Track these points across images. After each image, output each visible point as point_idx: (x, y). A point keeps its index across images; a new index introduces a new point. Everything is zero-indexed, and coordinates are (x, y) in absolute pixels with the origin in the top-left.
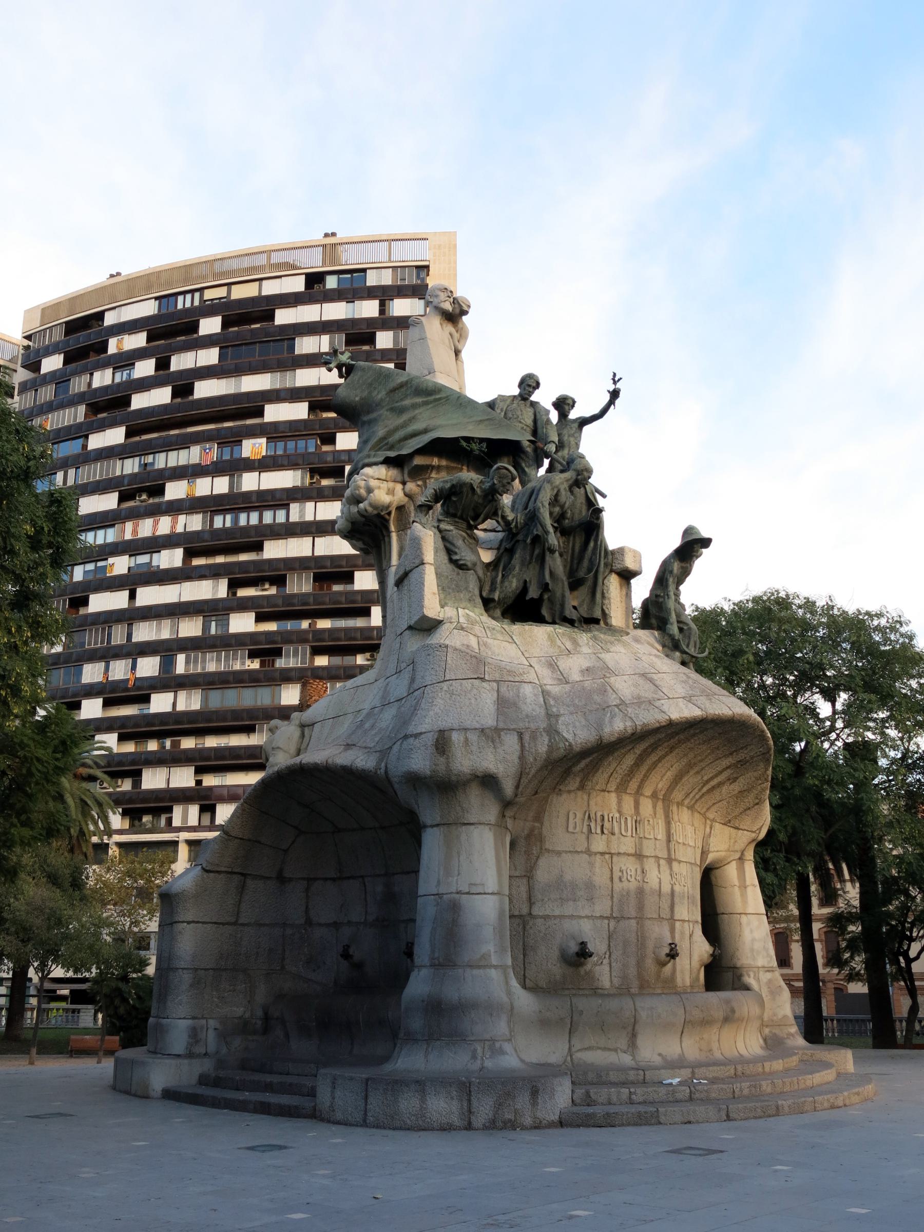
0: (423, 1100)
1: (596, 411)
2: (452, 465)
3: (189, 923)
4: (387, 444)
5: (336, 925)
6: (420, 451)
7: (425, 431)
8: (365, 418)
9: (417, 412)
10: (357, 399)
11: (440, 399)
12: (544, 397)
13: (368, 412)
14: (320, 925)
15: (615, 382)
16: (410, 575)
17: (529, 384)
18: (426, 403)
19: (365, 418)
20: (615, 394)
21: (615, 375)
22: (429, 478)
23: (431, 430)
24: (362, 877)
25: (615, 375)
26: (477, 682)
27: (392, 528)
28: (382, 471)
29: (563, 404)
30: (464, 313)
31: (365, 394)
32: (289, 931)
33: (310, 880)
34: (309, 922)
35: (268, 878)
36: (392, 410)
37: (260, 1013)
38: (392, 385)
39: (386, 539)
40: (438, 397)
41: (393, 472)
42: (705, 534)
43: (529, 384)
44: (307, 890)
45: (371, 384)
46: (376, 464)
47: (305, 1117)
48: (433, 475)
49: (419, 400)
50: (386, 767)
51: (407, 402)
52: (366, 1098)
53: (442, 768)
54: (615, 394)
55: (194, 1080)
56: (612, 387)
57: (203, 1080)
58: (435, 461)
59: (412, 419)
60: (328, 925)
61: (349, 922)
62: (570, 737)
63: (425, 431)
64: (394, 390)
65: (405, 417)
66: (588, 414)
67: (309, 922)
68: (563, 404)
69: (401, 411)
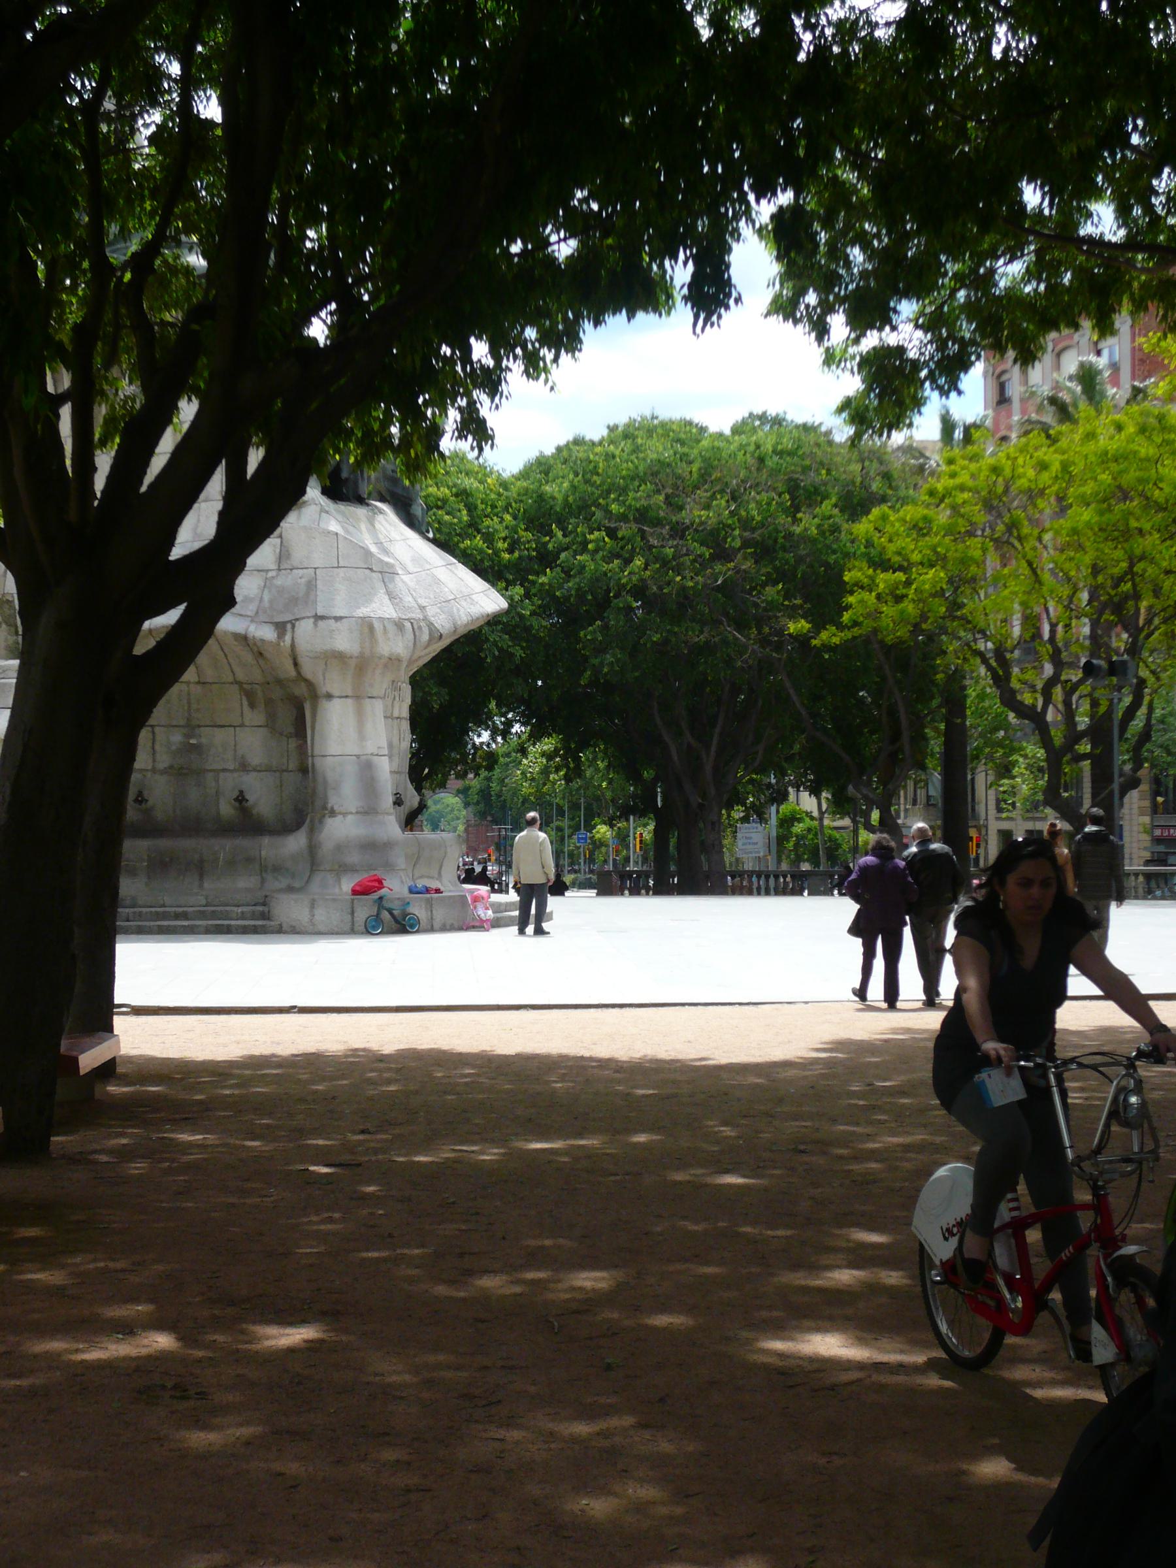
26: (367, 571)
47: (272, 932)
52: (353, 913)
53: (367, 652)
62: (439, 627)
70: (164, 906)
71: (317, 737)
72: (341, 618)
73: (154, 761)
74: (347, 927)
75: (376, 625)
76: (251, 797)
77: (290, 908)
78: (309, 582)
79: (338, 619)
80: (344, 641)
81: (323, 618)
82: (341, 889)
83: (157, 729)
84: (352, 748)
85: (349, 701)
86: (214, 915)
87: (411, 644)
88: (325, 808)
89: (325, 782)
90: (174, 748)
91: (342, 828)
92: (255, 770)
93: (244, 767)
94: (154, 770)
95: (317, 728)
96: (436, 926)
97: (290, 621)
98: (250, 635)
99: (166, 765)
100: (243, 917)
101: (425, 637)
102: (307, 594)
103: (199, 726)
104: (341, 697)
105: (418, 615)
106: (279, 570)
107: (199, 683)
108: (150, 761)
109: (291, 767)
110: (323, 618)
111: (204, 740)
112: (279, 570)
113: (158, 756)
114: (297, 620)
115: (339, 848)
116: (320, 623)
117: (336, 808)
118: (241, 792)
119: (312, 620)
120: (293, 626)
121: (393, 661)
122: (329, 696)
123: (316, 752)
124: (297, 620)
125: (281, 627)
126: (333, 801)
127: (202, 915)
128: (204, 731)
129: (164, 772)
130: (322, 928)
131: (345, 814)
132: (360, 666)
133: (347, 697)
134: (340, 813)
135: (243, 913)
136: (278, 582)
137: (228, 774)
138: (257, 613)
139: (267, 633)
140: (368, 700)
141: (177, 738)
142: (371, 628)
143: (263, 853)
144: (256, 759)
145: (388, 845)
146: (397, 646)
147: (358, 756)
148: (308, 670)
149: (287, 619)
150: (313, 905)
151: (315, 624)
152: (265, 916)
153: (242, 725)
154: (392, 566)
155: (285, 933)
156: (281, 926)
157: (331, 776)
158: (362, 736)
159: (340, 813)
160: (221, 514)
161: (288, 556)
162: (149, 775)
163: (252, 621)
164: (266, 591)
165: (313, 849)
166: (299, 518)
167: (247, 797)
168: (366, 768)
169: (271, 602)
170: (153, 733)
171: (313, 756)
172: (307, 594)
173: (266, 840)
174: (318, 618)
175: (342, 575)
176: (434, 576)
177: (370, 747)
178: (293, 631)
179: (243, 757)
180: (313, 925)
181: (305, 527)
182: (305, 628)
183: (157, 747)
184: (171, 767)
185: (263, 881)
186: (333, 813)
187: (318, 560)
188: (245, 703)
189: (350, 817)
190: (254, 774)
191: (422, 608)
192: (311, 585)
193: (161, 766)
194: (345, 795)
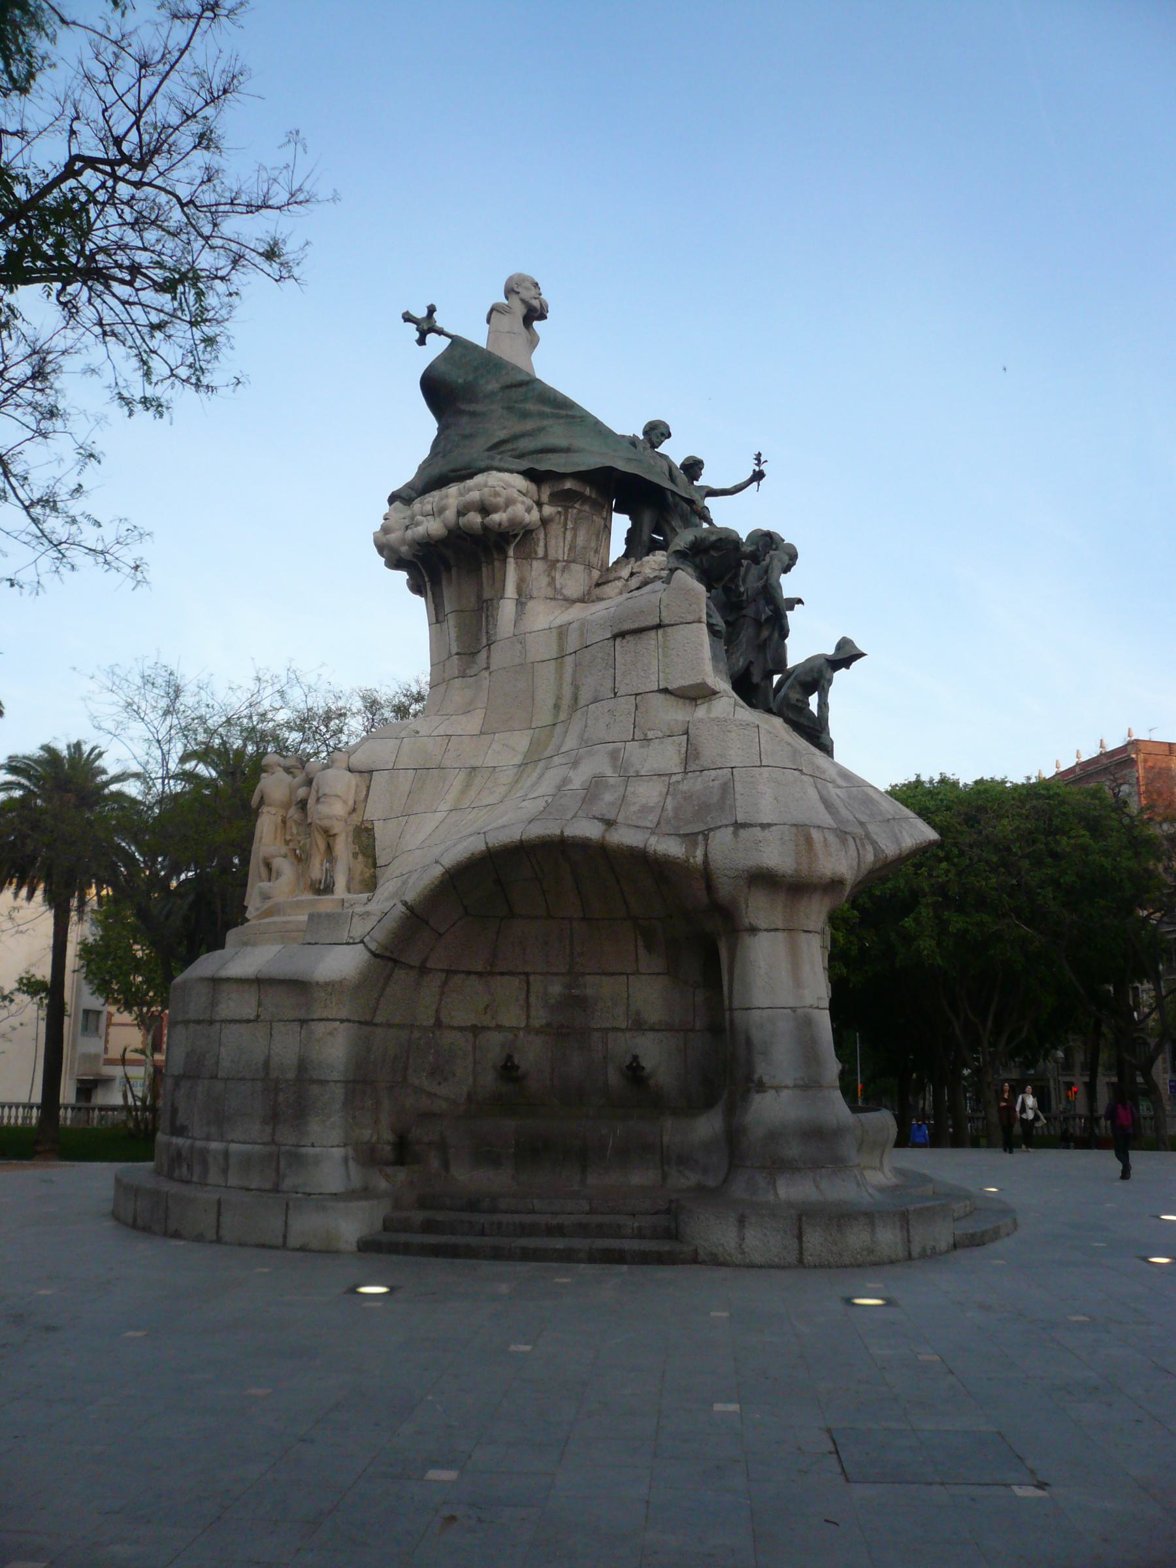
0: (873, 1233)
1: (728, 485)
2: (600, 500)
3: (342, 1021)
4: (513, 450)
5: (476, 1030)
6: (578, 476)
7: (567, 450)
8: (464, 407)
9: (545, 423)
10: (460, 381)
11: (573, 417)
12: (675, 451)
13: (471, 401)
14: (453, 1028)
15: (758, 465)
16: (669, 630)
17: (657, 432)
18: (558, 417)
19: (464, 407)
20: (758, 476)
21: (759, 454)
22: (572, 507)
23: (575, 452)
24: (527, 974)
25: (759, 454)
27: (511, 553)
28: (519, 482)
29: (693, 467)
30: (542, 316)
31: (470, 378)
32: (416, 1034)
33: (450, 973)
34: (438, 1024)
35: (412, 967)
36: (510, 409)
37: (388, 1136)
38: (508, 380)
39: (497, 564)
40: (570, 413)
41: (532, 487)
42: (861, 646)
43: (657, 432)
44: (445, 984)
45: (476, 369)
46: (511, 471)
47: (683, 1262)
48: (577, 506)
49: (548, 410)
50: (706, 855)
51: (531, 407)
52: (800, 1237)
54: (758, 476)
55: (379, 1225)
56: (757, 469)
57: (388, 1226)
58: (588, 492)
59: (541, 430)
60: (462, 1029)
61: (499, 1028)
62: (884, 847)
63: (567, 450)
64: (510, 387)
65: (529, 425)
66: (716, 485)
67: (438, 1024)
68: (693, 467)
69: (525, 415)
70: (533, 1212)
71: (736, 987)
72: (769, 825)
73: (528, 1017)
74: (792, 1258)
75: (816, 834)
76: (647, 1063)
77: (716, 1232)
78: (725, 784)
79: (764, 826)
80: (775, 855)
81: (744, 826)
82: (776, 1194)
83: (532, 978)
84: (786, 998)
85: (780, 936)
86: (601, 1231)
87: (855, 863)
88: (749, 1078)
89: (749, 1042)
90: (552, 1001)
91: (774, 1108)
92: (652, 1029)
93: (639, 1026)
94: (528, 1028)
95: (737, 972)
96: (915, 1254)
97: (702, 832)
98: (651, 849)
99: (544, 1022)
100: (640, 1235)
101: (870, 857)
102: (723, 798)
103: (584, 974)
104: (766, 930)
105: (859, 831)
106: (685, 773)
107: (583, 919)
108: (524, 1017)
109: (698, 1025)
110: (744, 826)
111: (589, 991)
112: (685, 773)
113: (533, 1013)
114: (711, 830)
115: (774, 1136)
116: (743, 833)
117: (766, 1079)
118: (635, 1058)
119: (731, 829)
120: (706, 838)
121: (835, 884)
122: (753, 930)
123: (736, 1004)
124: (711, 830)
125: (690, 838)
126: (761, 1070)
127: (583, 1230)
128: (590, 979)
129: (538, 1032)
130: (757, 1258)
131: (778, 1089)
132: (792, 888)
133: (776, 930)
134: (772, 1087)
135: (640, 1228)
136: (684, 787)
137: (619, 1034)
138: (658, 823)
139: (672, 848)
140: (803, 936)
141: (556, 989)
142: (809, 840)
143: (666, 1139)
144: (654, 1014)
145: (838, 1132)
146: (840, 863)
147: (793, 1009)
148: (725, 889)
149: (696, 831)
150: (742, 1221)
151: (735, 834)
152: (673, 1234)
153: (637, 973)
154: (824, 772)
155: (703, 1262)
156: (696, 1252)
157: (757, 1036)
158: (798, 983)
159: (772, 1087)
160: (629, 531)
161: (697, 756)
162: (521, 1033)
163: (653, 833)
164: (669, 798)
165: (733, 1139)
166: (709, 711)
167: (644, 1064)
168: (806, 1023)
169: (677, 810)
170: (528, 983)
171: (731, 1010)
172: (723, 798)
173: (669, 1123)
174: (738, 826)
175: (766, 775)
176: (867, 795)
177: (809, 1000)
178: (706, 845)
179: (638, 1013)
180: (743, 1253)
181: (717, 720)
182: (722, 841)
183: (533, 999)
184: (548, 1025)
185: (665, 1177)
186: (761, 1087)
187: (735, 757)
188: (640, 943)
189: (785, 1093)
190: (651, 1035)
191: (862, 824)
192: (727, 788)
193: (536, 1023)
194: (780, 1062)
